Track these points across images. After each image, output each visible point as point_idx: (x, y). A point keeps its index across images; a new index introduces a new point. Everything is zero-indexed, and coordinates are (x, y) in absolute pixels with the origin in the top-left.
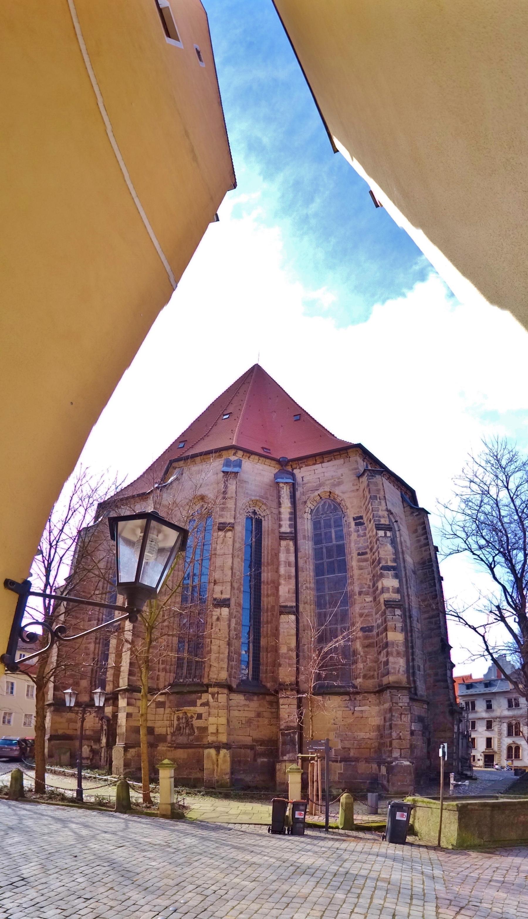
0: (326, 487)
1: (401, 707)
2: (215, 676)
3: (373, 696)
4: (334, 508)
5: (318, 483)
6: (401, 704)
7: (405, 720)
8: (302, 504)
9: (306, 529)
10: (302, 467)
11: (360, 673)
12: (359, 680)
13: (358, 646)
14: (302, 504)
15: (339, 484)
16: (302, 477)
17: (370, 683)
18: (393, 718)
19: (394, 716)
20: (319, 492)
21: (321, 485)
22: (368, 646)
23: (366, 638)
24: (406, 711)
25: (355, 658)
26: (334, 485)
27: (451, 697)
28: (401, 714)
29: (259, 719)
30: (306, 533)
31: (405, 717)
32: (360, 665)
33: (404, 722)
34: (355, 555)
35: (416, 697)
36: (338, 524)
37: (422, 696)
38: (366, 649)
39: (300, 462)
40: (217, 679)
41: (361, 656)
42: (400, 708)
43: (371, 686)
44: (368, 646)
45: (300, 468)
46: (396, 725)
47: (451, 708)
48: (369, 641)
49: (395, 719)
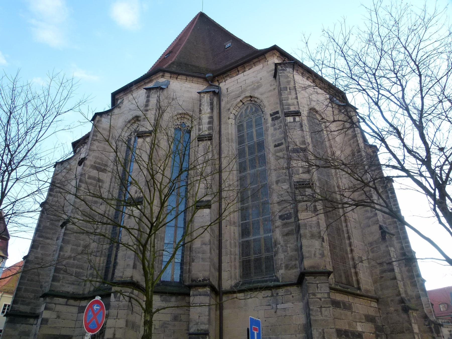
0: (247, 93)
1: (320, 299)
2: (121, 275)
3: (295, 287)
4: (255, 111)
5: (241, 90)
6: (319, 296)
7: (326, 314)
8: (226, 111)
9: (230, 132)
10: (227, 80)
11: (281, 264)
12: (282, 272)
13: (278, 235)
14: (226, 111)
15: (258, 87)
16: (227, 89)
17: (293, 275)
18: (311, 312)
19: (312, 310)
20: (241, 98)
21: (242, 92)
22: (287, 234)
23: (285, 225)
24: (327, 304)
25: (276, 248)
26: (254, 89)
27: (401, 290)
28: (321, 307)
29: (176, 323)
30: (230, 136)
31: (326, 310)
32: (281, 256)
33: (326, 316)
34: (272, 148)
35: (358, 292)
36: (258, 123)
37: (367, 291)
38: (286, 238)
39: (224, 76)
40: (122, 277)
41: (282, 246)
42: (319, 300)
43: (293, 277)
44: (287, 234)
45: (225, 81)
46: (316, 320)
47: (403, 304)
48: (288, 228)
49: (314, 314)
